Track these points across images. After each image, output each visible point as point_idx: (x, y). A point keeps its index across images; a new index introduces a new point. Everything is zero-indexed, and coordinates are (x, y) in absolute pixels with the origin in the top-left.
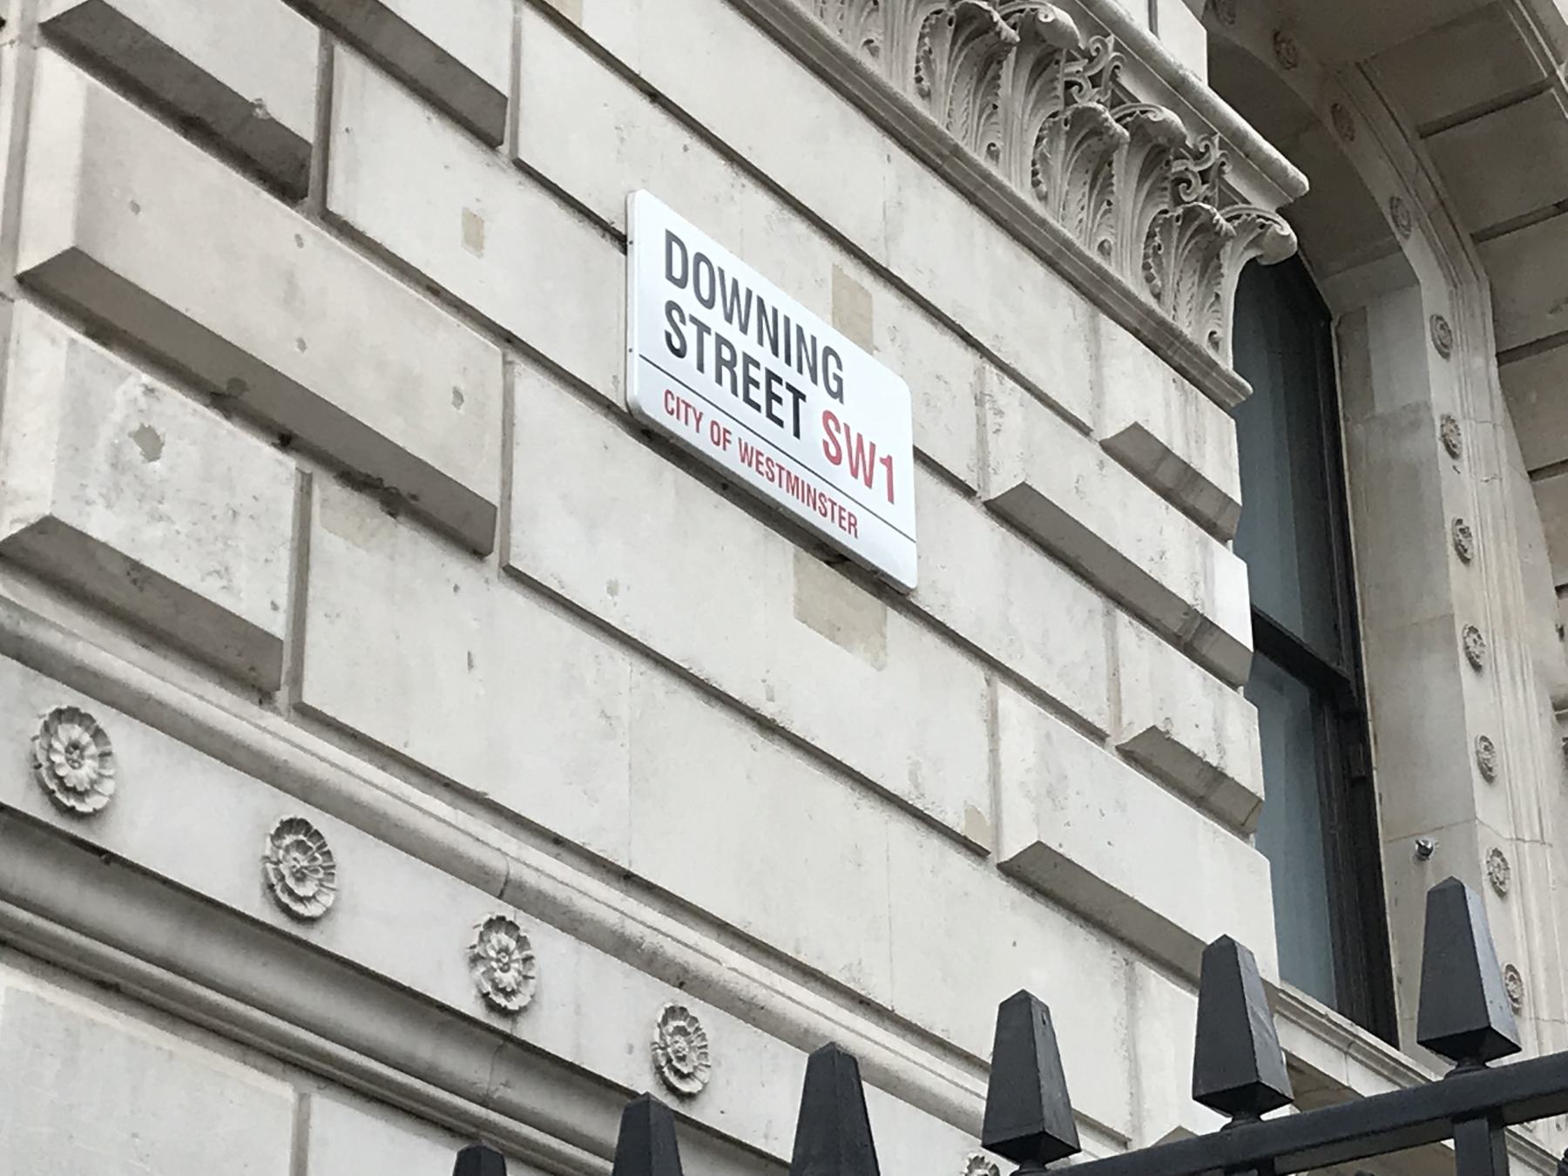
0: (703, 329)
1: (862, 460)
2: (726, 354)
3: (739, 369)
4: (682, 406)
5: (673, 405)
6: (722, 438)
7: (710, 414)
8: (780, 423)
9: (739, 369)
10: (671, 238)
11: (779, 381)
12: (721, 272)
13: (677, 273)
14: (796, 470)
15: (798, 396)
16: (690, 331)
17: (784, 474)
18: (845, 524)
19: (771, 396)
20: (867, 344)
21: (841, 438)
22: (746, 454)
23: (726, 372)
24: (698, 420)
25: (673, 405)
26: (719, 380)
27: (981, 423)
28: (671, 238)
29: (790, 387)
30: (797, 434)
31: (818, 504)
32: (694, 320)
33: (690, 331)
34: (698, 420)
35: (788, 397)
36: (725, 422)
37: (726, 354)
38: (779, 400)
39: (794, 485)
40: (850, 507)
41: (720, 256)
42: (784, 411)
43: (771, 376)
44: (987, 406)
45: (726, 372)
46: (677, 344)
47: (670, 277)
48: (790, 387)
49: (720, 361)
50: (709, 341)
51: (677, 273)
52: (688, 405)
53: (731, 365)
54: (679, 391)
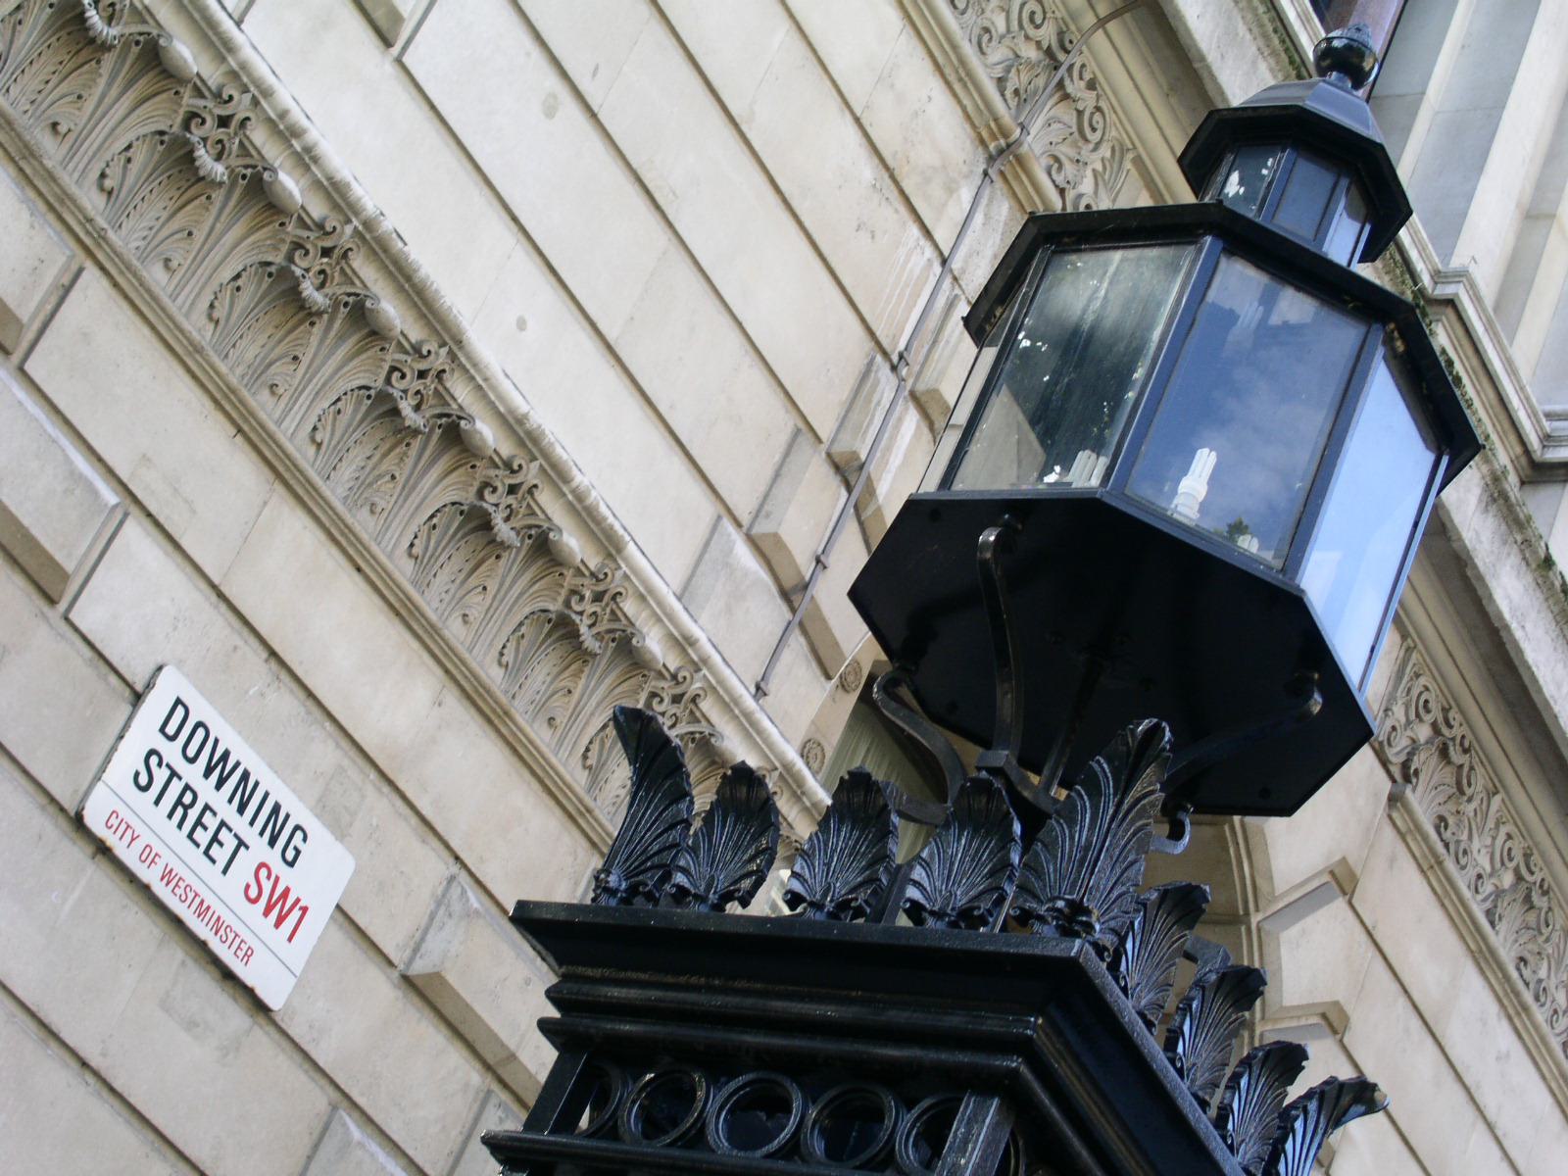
0: (174, 774)
1: (281, 906)
2: (188, 798)
3: (193, 814)
4: (123, 827)
5: (114, 821)
6: (149, 857)
7: (146, 838)
8: (213, 861)
9: (193, 814)
10: (178, 702)
11: (230, 830)
12: (216, 741)
13: (171, 730)
14: (210, 900)
15: (241, 843)
16: (161, 775)
17: (197, 901)
18: (241, 954)
19: (215, 839)
20: (340, 831)
21: (267, 886)
22: (168, 876)
23: (180, 811)
24: (133, 840)
25: (114, 821)
26: (170, 816)
27: (432, 917)
28: (178, 702)
29: (236, 835)
30: (225, 872)
31: (222, 932)
32: (168, 766)
33: (161, 775)
34: (133, 840)
35: (230, 842)
36: (157, 847)
37: (188, 798)
38: (221, 844)
39: (203, 911)
40: (252, 941)
41: (219, 728)
42: (221, 854)
43: (223, 824)
44: (443, 908)
45: (180, 811)
46: (143, 780)
47: (162, 730)
48: (236, 835)
49: (179, 802)
50: (176, 787)
51: (171, 730)
52: (128, 826)
53: (186, 808)
54: (124, 813)
